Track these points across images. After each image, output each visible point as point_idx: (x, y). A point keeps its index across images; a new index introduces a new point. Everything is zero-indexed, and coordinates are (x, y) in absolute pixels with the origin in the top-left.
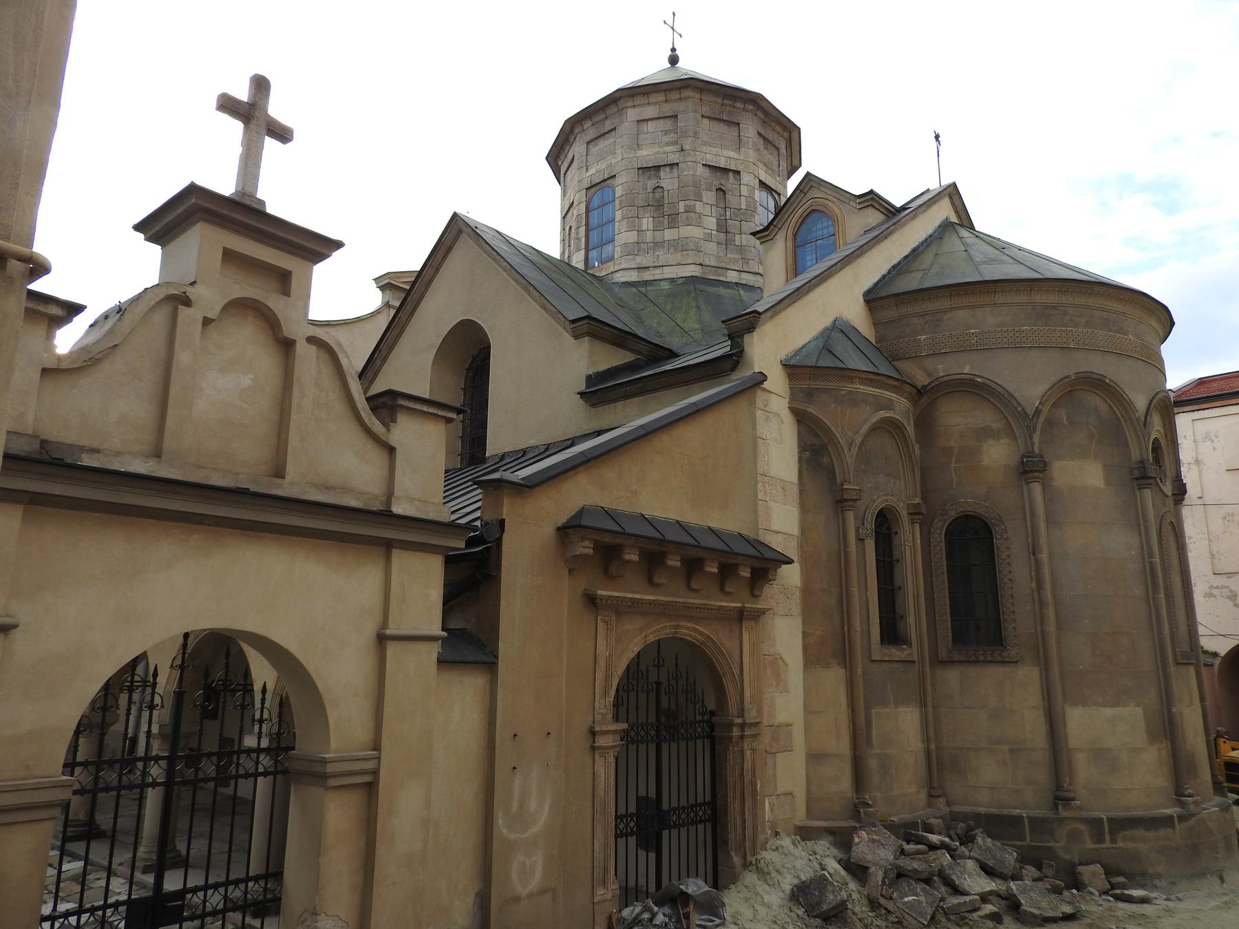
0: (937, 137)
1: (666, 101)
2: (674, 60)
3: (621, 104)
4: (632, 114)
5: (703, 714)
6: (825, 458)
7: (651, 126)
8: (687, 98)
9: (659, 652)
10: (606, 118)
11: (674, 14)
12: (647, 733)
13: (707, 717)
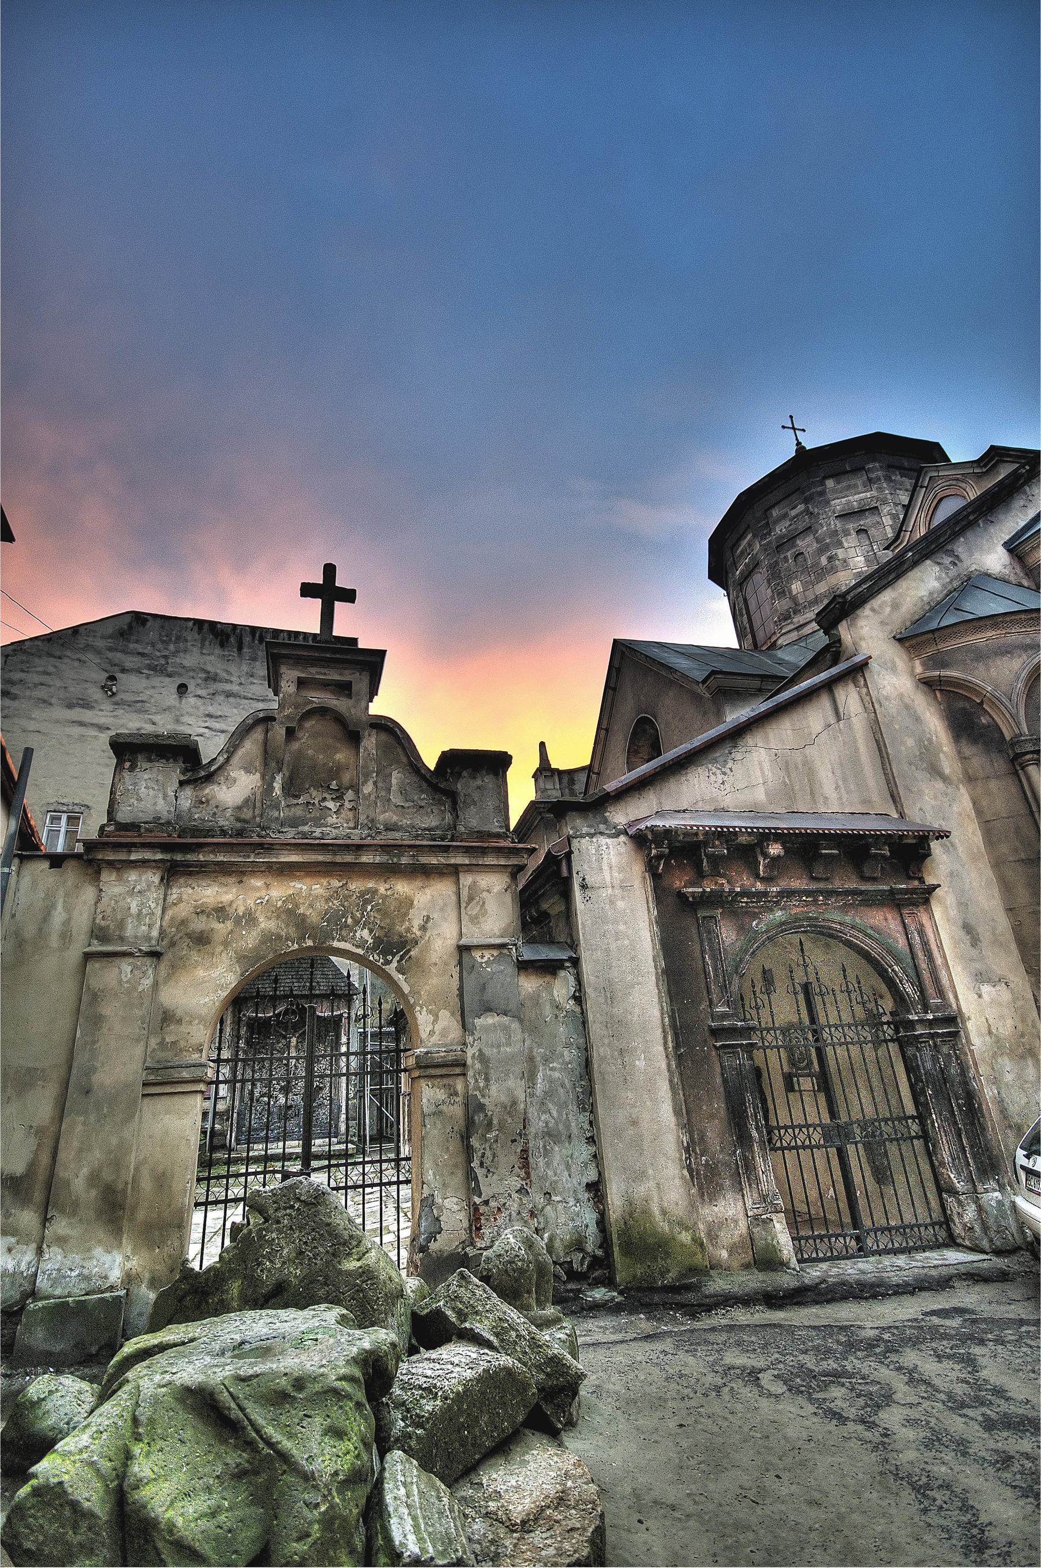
6: (982, 718)
11: (791, 417)
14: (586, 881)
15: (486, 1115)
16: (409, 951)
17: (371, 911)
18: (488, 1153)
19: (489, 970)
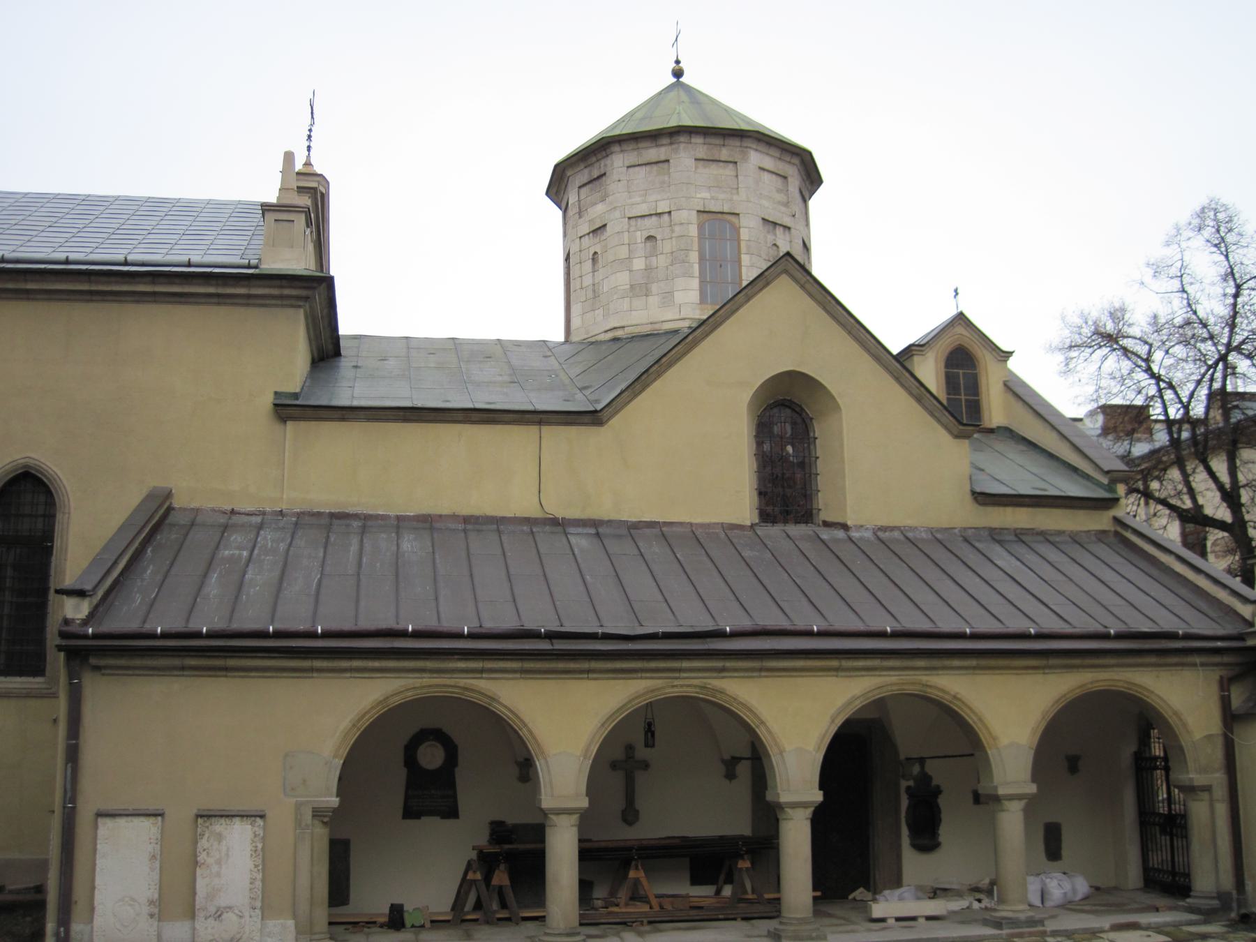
0: (956, 291)
1: (780, 159)
2: (678, 73)
3: (747, 143)
4: (756, 158)
7: (766, 176)
8: (794, 164)
10: (724, 145)
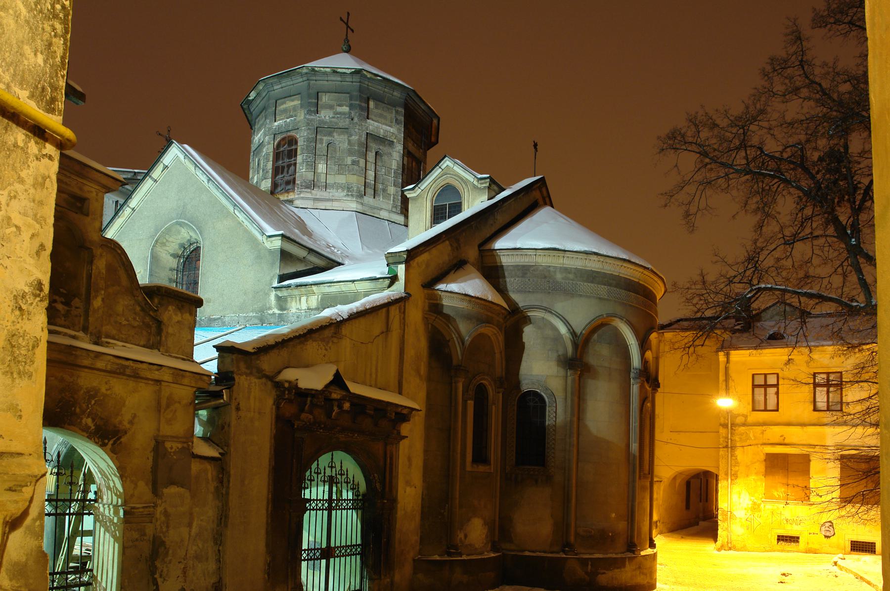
5: (358, 496)
9: (332, 459)
11: (348, 13)
12: (323, 505)
13: (360, 498)
14: (241, 405)
15: (165, 548)
16: (120, 437)
17: (95, 404)
18: (165, 570)
19: (175, 457)
